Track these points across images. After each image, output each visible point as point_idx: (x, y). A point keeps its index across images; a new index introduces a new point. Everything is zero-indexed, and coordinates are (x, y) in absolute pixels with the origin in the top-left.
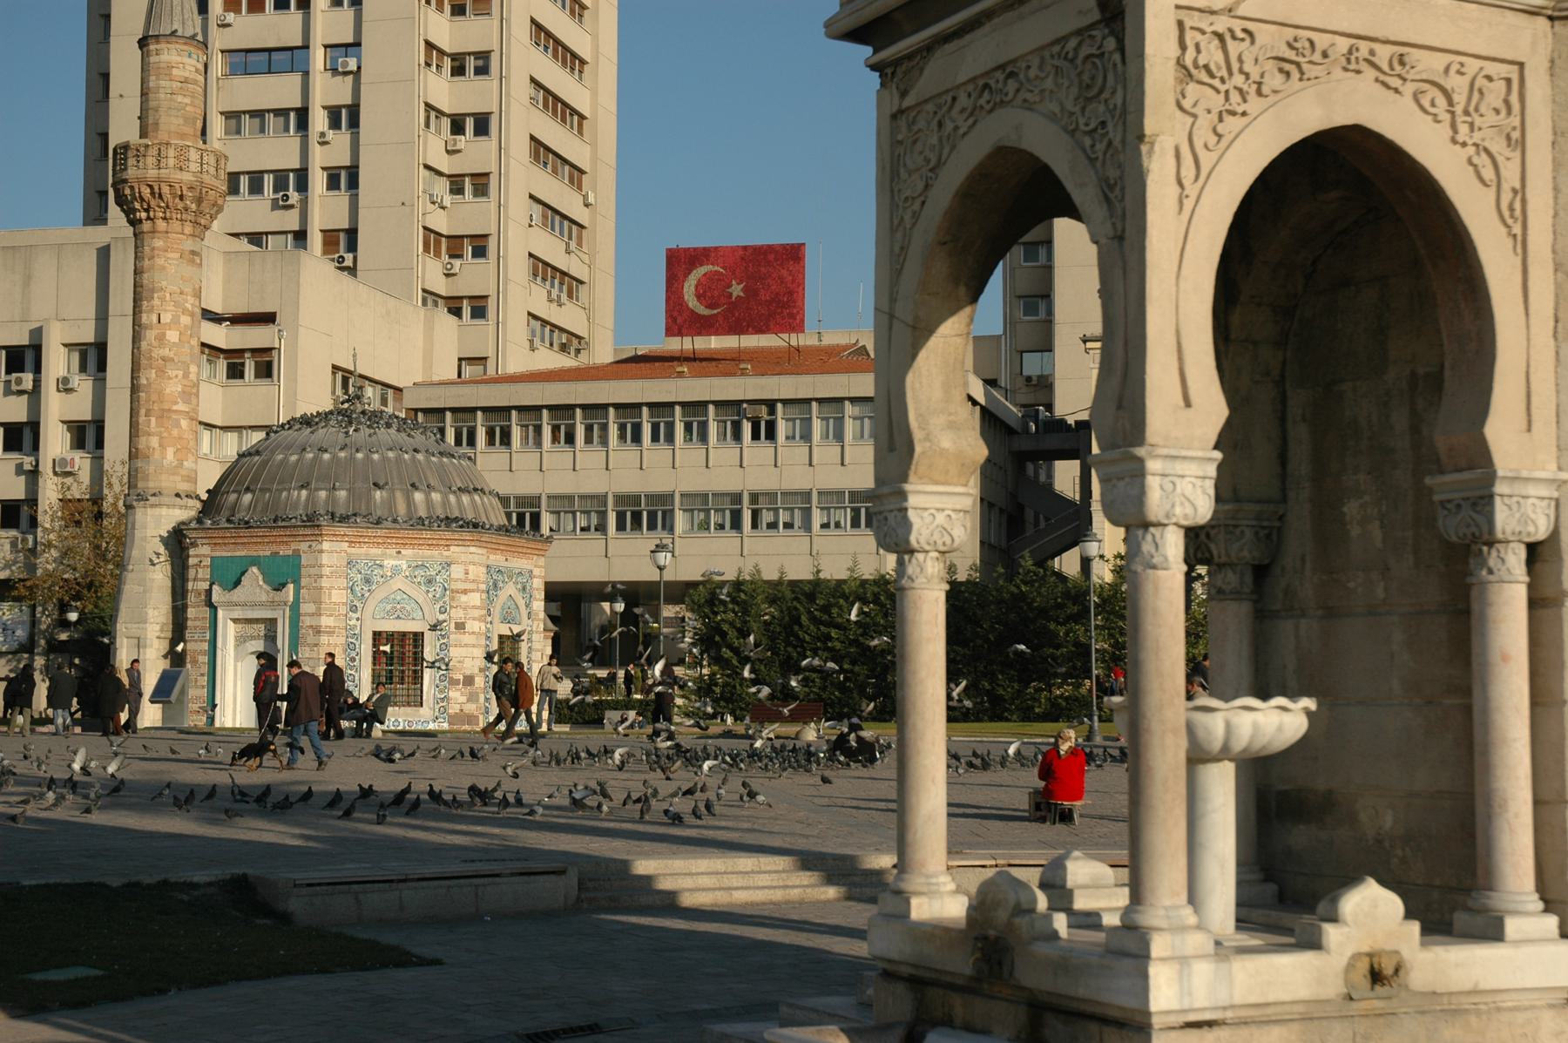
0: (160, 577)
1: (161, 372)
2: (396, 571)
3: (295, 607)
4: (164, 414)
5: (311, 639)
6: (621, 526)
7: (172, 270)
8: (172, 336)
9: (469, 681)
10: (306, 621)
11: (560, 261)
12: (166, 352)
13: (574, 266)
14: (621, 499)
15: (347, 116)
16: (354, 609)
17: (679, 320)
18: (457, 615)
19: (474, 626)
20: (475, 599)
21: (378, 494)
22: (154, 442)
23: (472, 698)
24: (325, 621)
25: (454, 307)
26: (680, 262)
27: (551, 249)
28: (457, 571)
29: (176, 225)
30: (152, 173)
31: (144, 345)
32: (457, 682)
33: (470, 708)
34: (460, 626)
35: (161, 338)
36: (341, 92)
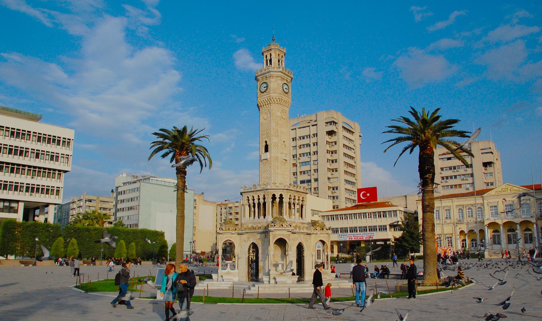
15: (316, 171)
36: (315, 167)
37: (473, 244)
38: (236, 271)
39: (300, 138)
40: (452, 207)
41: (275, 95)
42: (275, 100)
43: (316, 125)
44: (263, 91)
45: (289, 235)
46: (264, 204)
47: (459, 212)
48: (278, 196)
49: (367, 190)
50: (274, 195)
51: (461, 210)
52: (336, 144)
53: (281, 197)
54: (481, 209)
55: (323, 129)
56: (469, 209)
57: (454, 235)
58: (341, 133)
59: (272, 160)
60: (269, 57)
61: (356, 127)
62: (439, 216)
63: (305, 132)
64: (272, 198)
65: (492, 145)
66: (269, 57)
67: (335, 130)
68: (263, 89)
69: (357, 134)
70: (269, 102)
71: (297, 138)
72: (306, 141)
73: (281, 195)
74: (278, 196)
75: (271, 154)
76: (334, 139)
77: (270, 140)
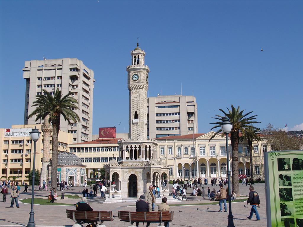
0: (46, 170)
1: (46, 149)
2: (71, 169)
3: (60, 173)
4: (47, 153)
5: (62, 177)
6: (94, 161)
7: (47, 138)
8: (48, 145)
9: (78, 181)
10: (62, 175)
11: (85, 125)
12: (47, 147)
13: (87, 126)
14: (93, 158)
16: (67, 174)
17: (101, 136)
18: (77, 174)
19: (79, 175)
20: (79, 172)
21: (69, 161)
22: (45, 156)
23: (79, 183)
24: (64, 175)
25: (72, 132)
26: (101, 129)
27: (85, 124)
28: (77, 169)
29: (47, 133)
30: (46, 128)
31: (44, 146)
32: (77, 181)
33: (78, 184)
34: (78, 175)
35: (46, 145)
37: (186, 173)
38: (120, 191)
39: (45, 78)
40: (174, 146)
41: (143, 83)
42: (143, 87)
43: (62, 69)
44: (135, 80)
45: (160, 170)
46: (140, 150)
47: (178, 150)
48: (148, 147)
50: (146, 146)
51: (180, 149)
52: (77, 87)
53: (150, 148)
54: (193, 149)
55: (67, 74)
56: (185, 148)
57: (174, 166)
58: (82, 78)
59: (141, 123)
60: (137, 58)
61: (91, 74)
62: (164, 152)
63: (51, 74)
64: (145, 148)
65: (194, 99)
66: (137, 58)
67: (78, 76)
68: (135, 79)
69: (92, 79)
70: (139, 87)
71: (43, 78)
72: (51, 82)
73: (150, 146)
74: (148, 147)
75: (140, 120)
76: (76, 83)
77: (139, 111)
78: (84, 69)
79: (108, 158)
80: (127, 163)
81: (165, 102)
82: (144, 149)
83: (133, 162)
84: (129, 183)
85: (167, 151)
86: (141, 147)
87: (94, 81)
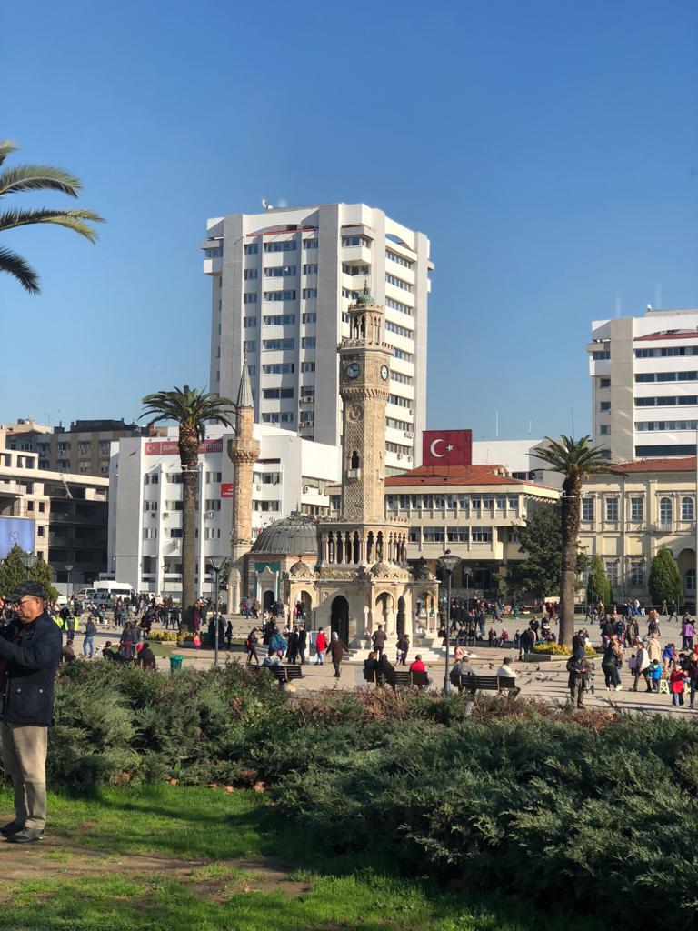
46: (357, 543)
48: (375, 534)
49: (447, 435)
50: (371, 533)
51: (666, 505)
56: (684, 500)
73: (380, 533)
74: (375, 534)
77: (362, 451)
78: (390, 237)
79: (468, 528)
80: (329, 570)
81: (671, 334)
82: (366, 540)
83: (343, 570)
84: (332, 616)
85: (626, 510)
86: (359, 534)
87: (429, 269)
